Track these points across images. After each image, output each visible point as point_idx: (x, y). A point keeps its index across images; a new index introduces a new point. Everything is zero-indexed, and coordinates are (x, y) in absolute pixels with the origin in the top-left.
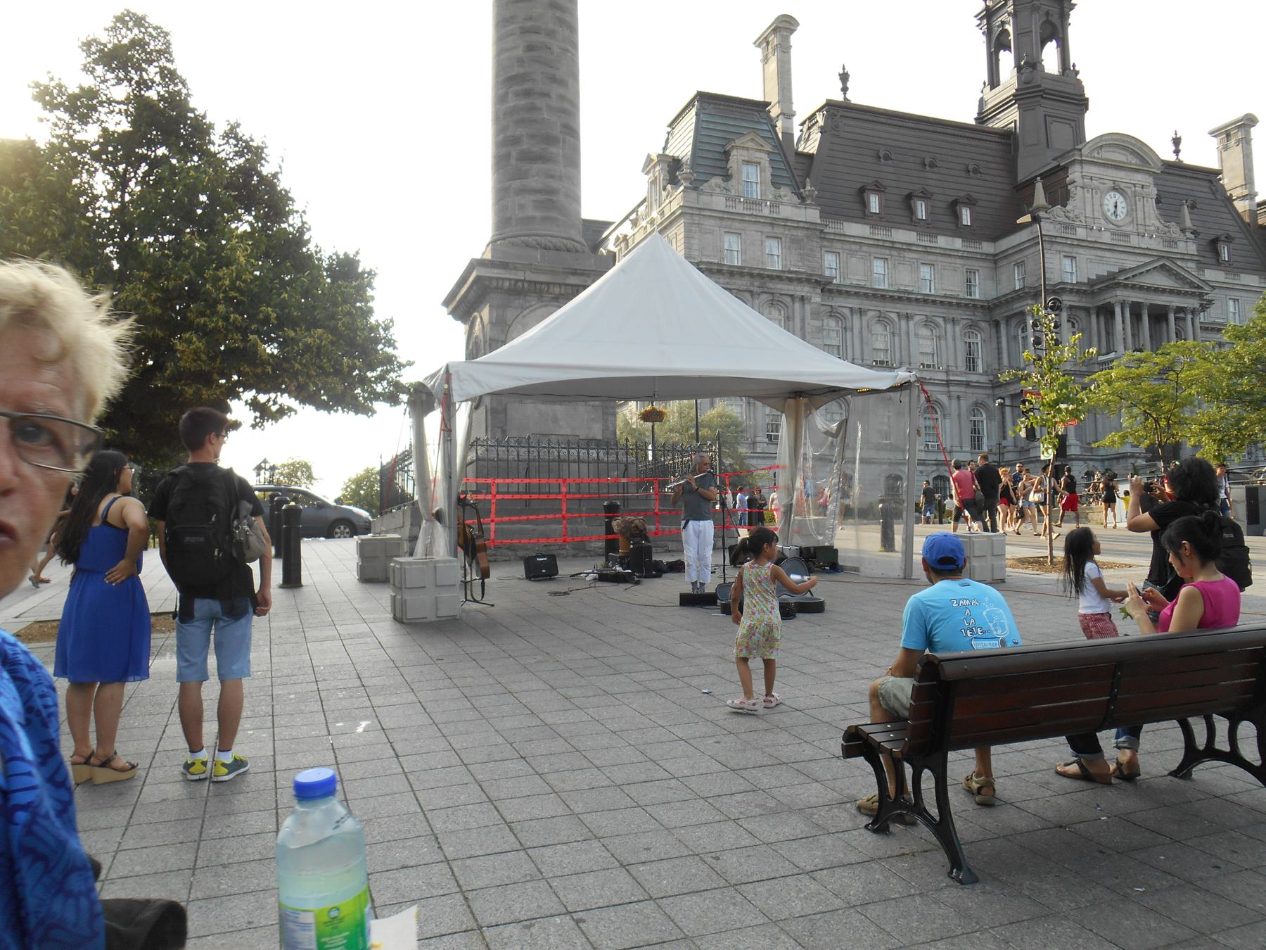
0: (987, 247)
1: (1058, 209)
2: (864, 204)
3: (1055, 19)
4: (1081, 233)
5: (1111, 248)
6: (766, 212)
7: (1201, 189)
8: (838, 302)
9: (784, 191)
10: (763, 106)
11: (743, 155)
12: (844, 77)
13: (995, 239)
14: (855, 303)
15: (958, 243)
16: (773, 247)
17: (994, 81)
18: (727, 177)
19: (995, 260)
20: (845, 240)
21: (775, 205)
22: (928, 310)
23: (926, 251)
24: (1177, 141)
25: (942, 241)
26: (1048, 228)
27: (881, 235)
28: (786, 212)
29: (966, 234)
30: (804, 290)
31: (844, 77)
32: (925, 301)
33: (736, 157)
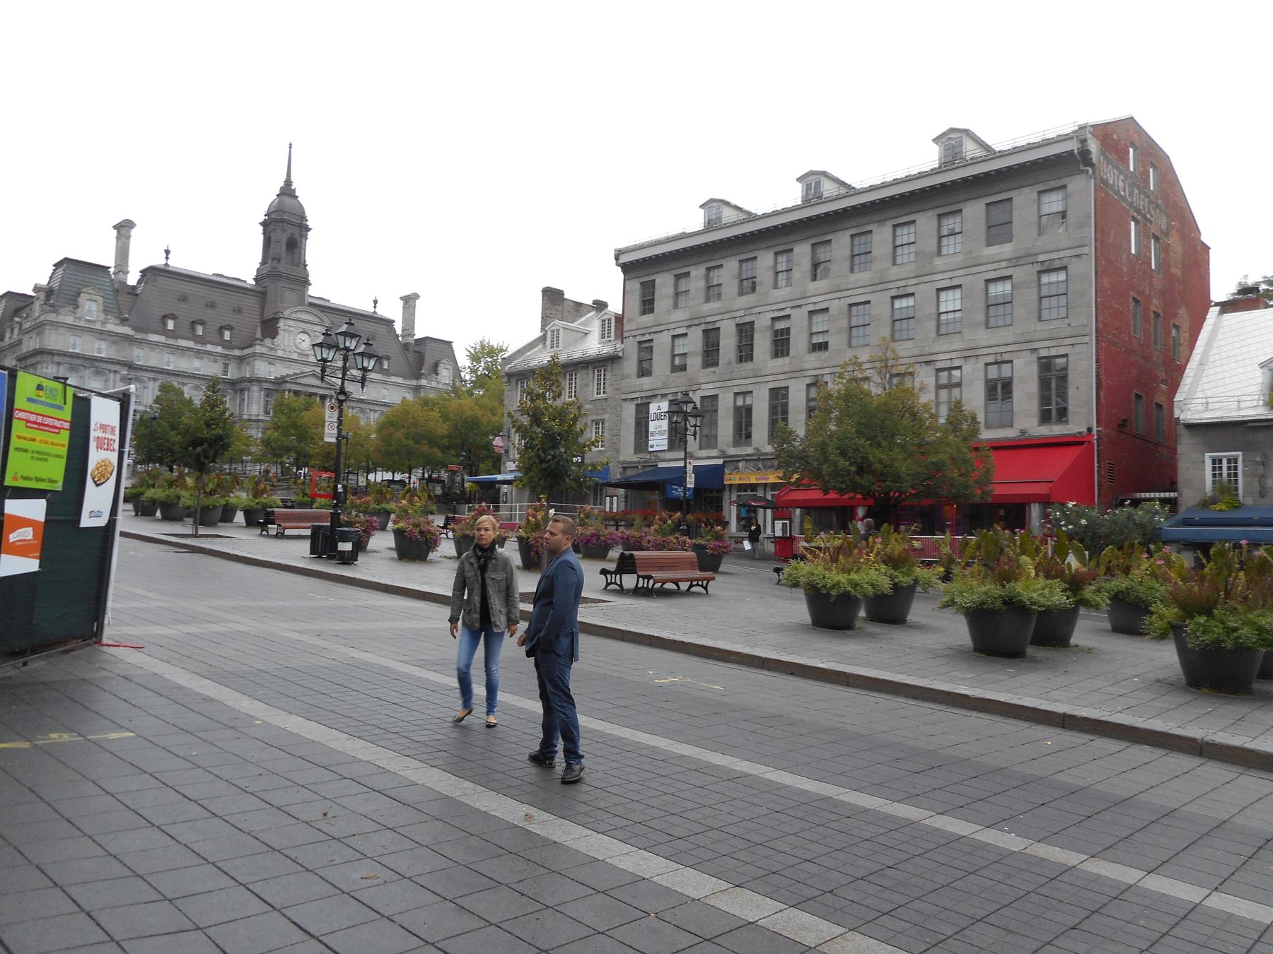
0: (237, 353)
1: (268, 341)
2: (165, 324)
3: (297, 236)
4: (280, 353)
5: (296, 361)
6: (98, 326)
7: (381, 330)
8: (140, 374)
9: (111, 319)
10: (106, 268)
11: (88, 297)
12: (167, 252)
13: (242, 349)
14: (152, 375)
15: (219, 349)
16: (103, 345)
17: (263, 263)
18: (77, 306)
19: (241, 359)
20: (150, 343)
21: (103, 323)
22: (197, 382)
23: (199, 351)
24: (376, 302)
25: (209, 348)
26: (258, 349)
27: (170, 342)
28: (110, 327)
29: (227, 345)
30: (117, 368)
31: (167, 252)
32: (193, 377)
33: (82, 299)
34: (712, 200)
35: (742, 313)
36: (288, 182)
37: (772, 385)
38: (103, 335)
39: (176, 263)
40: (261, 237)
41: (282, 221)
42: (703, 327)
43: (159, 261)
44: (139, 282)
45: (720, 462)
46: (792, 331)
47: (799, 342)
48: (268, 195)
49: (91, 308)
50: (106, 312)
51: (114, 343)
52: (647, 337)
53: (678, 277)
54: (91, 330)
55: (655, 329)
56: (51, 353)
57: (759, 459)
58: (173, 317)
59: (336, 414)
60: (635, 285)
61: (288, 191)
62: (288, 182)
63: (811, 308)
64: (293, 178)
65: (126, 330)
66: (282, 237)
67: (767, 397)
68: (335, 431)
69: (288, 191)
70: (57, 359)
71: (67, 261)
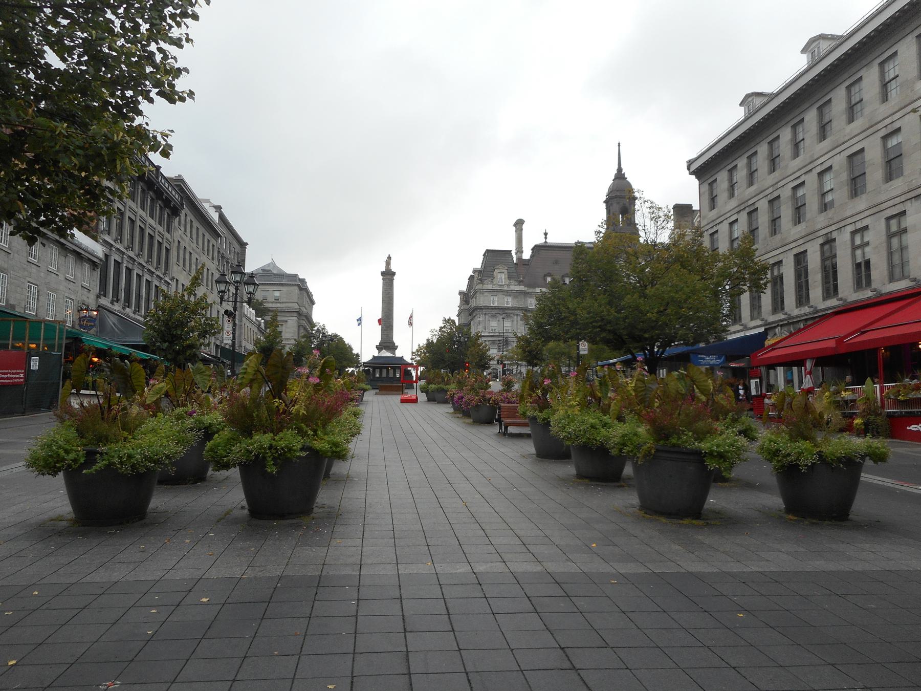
2: (545, 280)
3: (627, 205)
9: (513, 282)
12: (546, 234)
16: (510, 299)
21: (509, 285)
28: (513, 287)
30: (518, 312)
31: (546, 234)
34: (748, 96)
35: (771, 190)
36: (620, 170)
37: (795, 251)
38: (508, 293)
39: (551, 240)
40: (605, 211)
41: (616, 197)
42: (748, 210)
43: (541, 241)
44: (532, 256)
45: (762, 330)
46: (807, 197)
47: (812, 205)
48: (608, 180)
49: (501, 277)
50: (510, 278)
51: (515, 297)
52: (715, 229)
53: (731, 171)
54: (502, 291)
55: (718, 221)
56: (481, 308)
57: (789, 324)
58: (549, 275)
59: (231, 325)
60: (706, 187)
61: (620, 176)
62: (620, 170)
63: (819, 169)
64: (622, 167)
65: (522, 288)
66: (616, 207)
67: (793, 264)
68: (231, 336)
69: (620, 176)
70: (484, 311)
71: (488, 251)
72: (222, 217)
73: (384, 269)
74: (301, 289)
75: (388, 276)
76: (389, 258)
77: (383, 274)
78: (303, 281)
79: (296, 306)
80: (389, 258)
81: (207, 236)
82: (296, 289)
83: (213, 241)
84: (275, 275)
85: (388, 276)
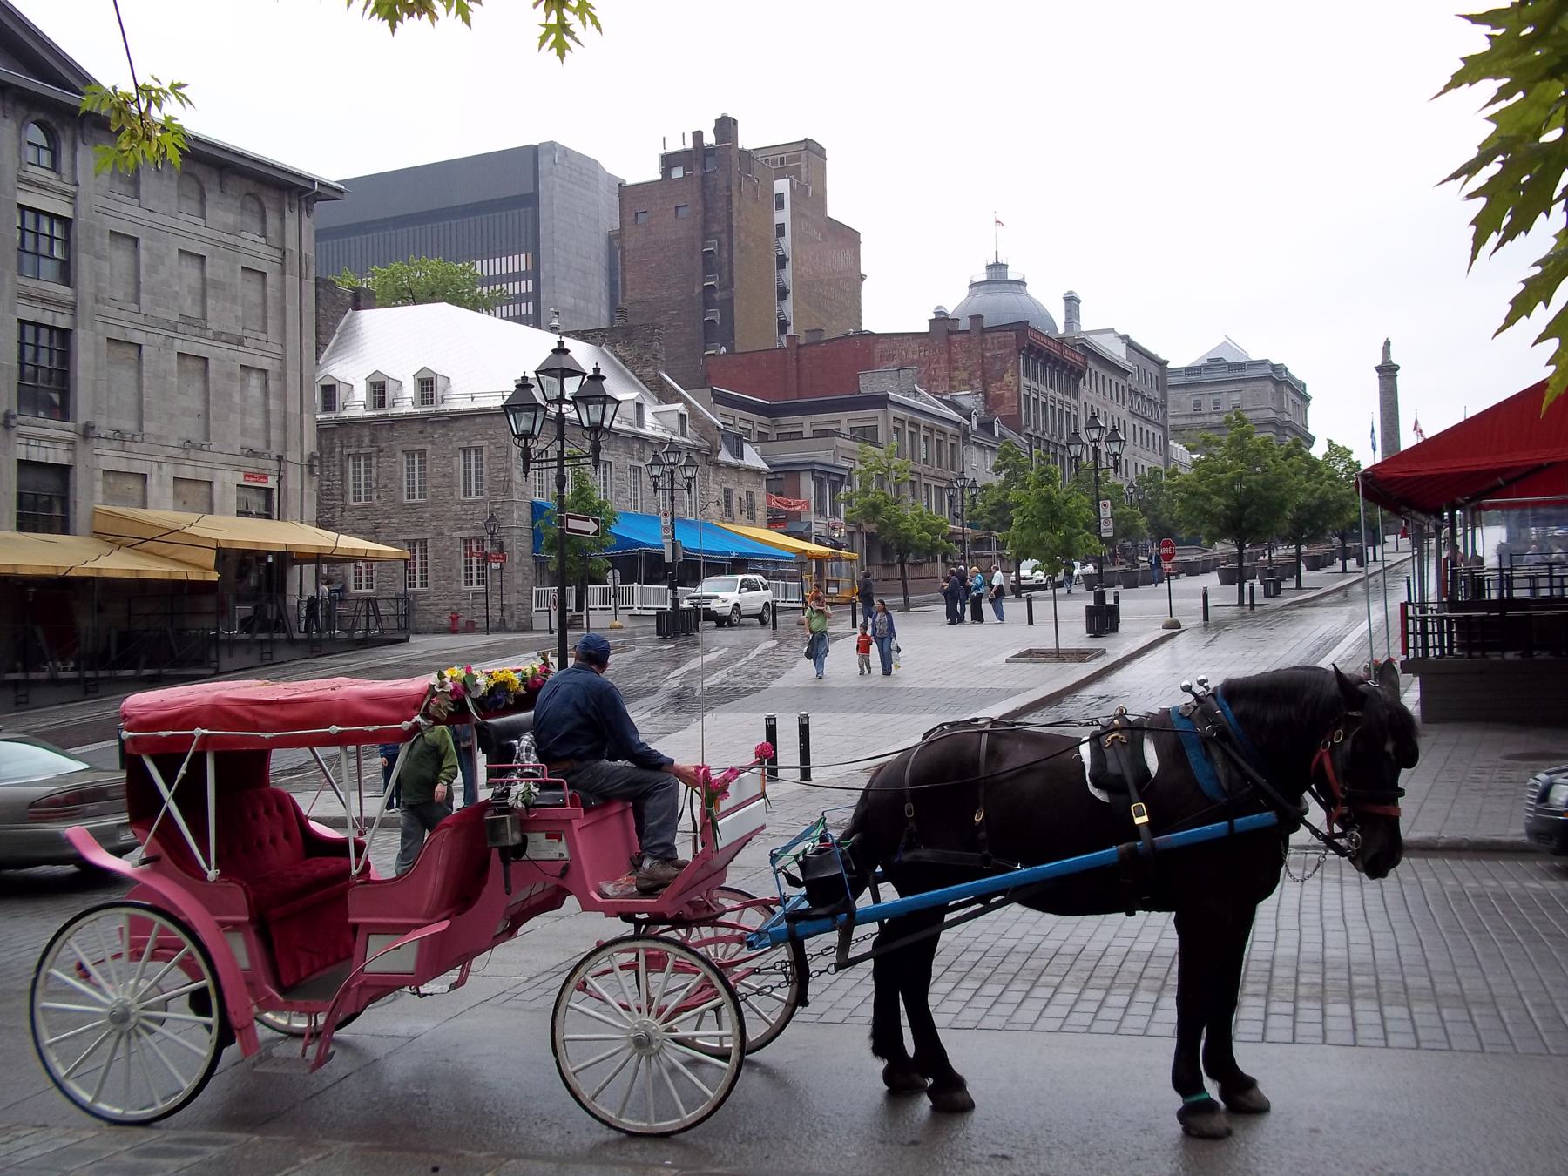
72: (1131, 345)
73: (1379, 363)
74: (1277, 383)
75: (1388, 371)
76: (1388, 344)
77: (1379, 369)
78: (1278, 368)
79: (1272, 414)
80: (1388, 344)
81: (1115, 379)
82: (1270, 387)
83: (1122, 382)
84: (1230, 365)
85: (1388, 371)
